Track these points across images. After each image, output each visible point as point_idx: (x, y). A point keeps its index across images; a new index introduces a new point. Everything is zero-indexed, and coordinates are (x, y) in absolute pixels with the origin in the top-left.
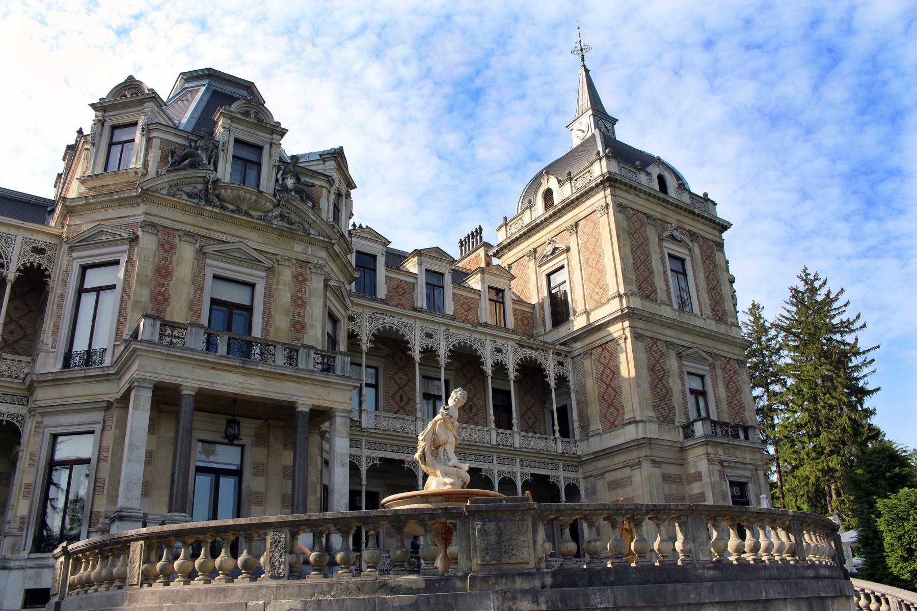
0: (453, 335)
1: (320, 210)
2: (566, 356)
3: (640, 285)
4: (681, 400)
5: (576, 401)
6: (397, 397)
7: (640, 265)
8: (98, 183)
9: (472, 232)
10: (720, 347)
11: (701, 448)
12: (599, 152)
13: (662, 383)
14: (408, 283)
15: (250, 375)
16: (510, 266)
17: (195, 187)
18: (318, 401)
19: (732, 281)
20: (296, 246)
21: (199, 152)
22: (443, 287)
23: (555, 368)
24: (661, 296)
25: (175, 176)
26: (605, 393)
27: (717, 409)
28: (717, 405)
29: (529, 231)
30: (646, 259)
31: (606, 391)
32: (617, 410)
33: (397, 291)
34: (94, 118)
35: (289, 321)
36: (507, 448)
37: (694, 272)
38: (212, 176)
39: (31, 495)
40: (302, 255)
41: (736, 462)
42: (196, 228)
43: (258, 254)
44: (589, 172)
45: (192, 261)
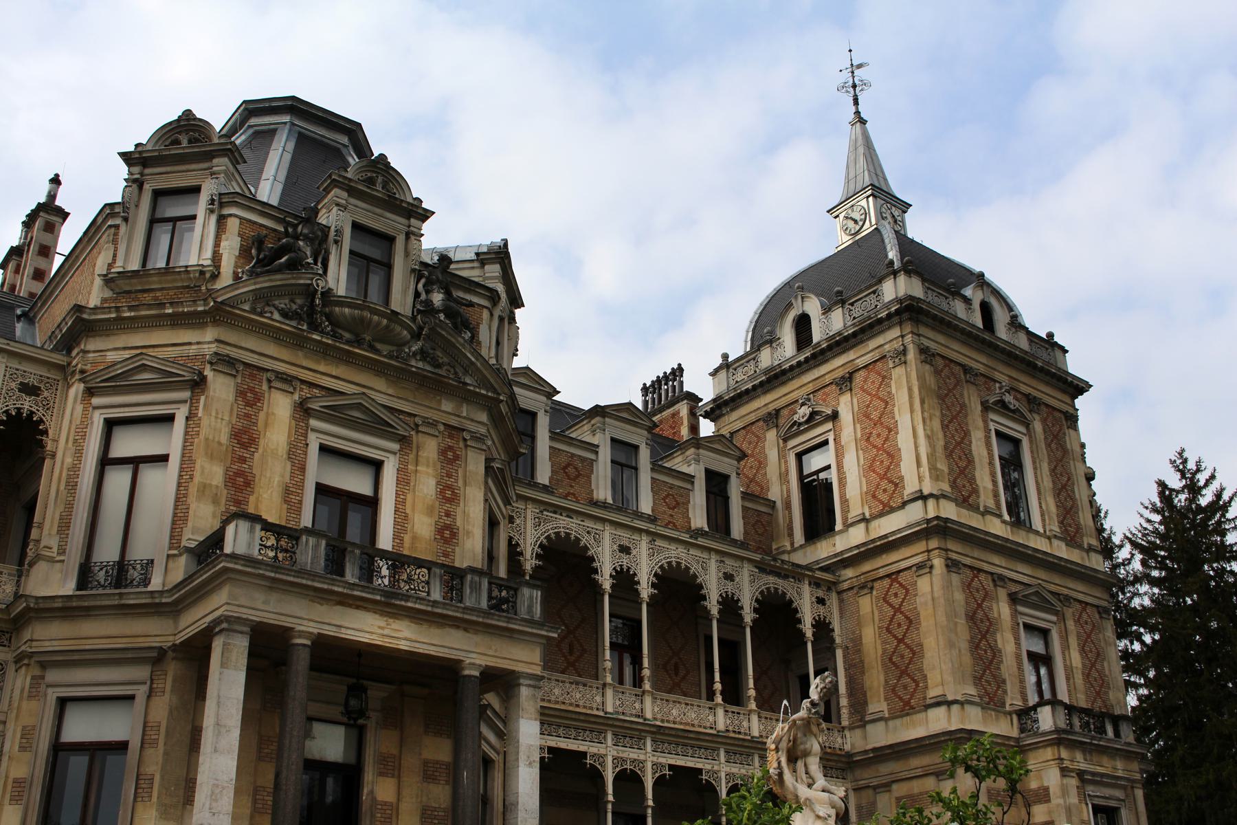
1: (479, 343)
2: (829, 589)
3: (954, 481)
4: (1015, 669)
5: (845, 662)
7: (955, 448)
9: (665, 373)
10: (1071, 585)
11: (1049, 750)
12: (892, 262)
13: (987, 641)
14: (583, 459)
15: (394, 616)
16: (732, 434)
17: (292, 301)
18: (494, 660)
19: (1090, 477)
20: (443, 401)
21: (301, 243)
22: (636, 469)
23: (812, 608)
24: (986, 500)
25: (264, 283)
26: (894, 652)
27: (1068, 685)
28: (1068, 679)
29: (769, 380)
30: (963, 439)
31: (896, 648)
32: (915, 681)
33: (566, 473)
34: (127, 177)
35: (433, 524)
36: (741, 736)
37: (1034, 462)
38: (321, 284)
39: (25, 798)
40: (453, 417)
41: (1102, 775)
42: (294, 368)
43: (389, 414)
44: (874, 292)
45: (288, 421)
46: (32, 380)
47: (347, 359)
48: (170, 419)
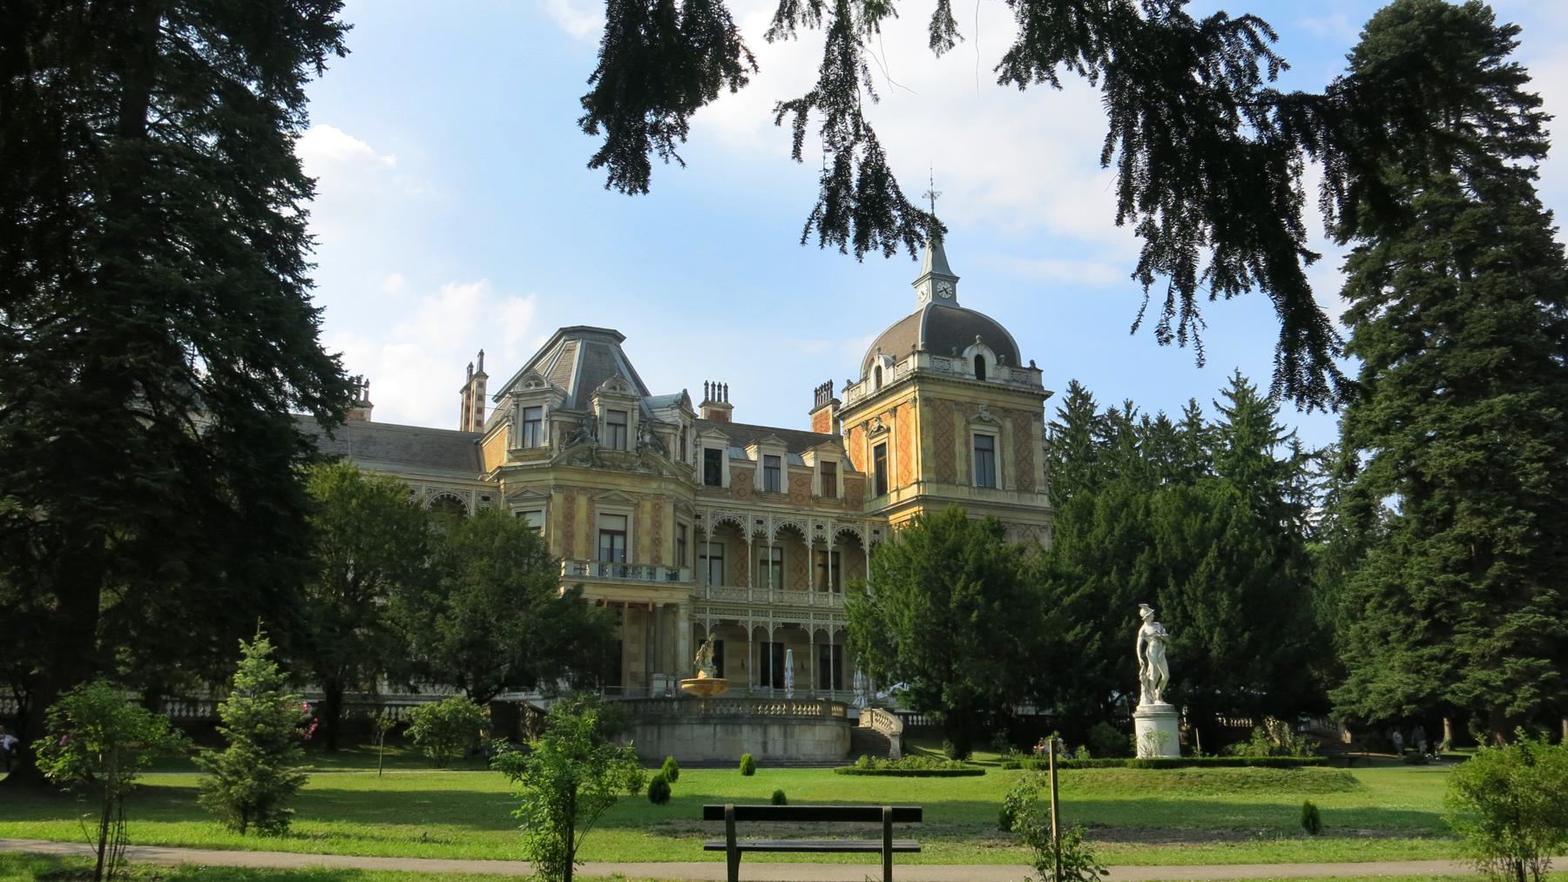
0: (780, 519)
6: (739, 566)
8: (521, 454)
22: (779, 469)
25: (571, 451)
46: (487, 495)
47: (610, 474)
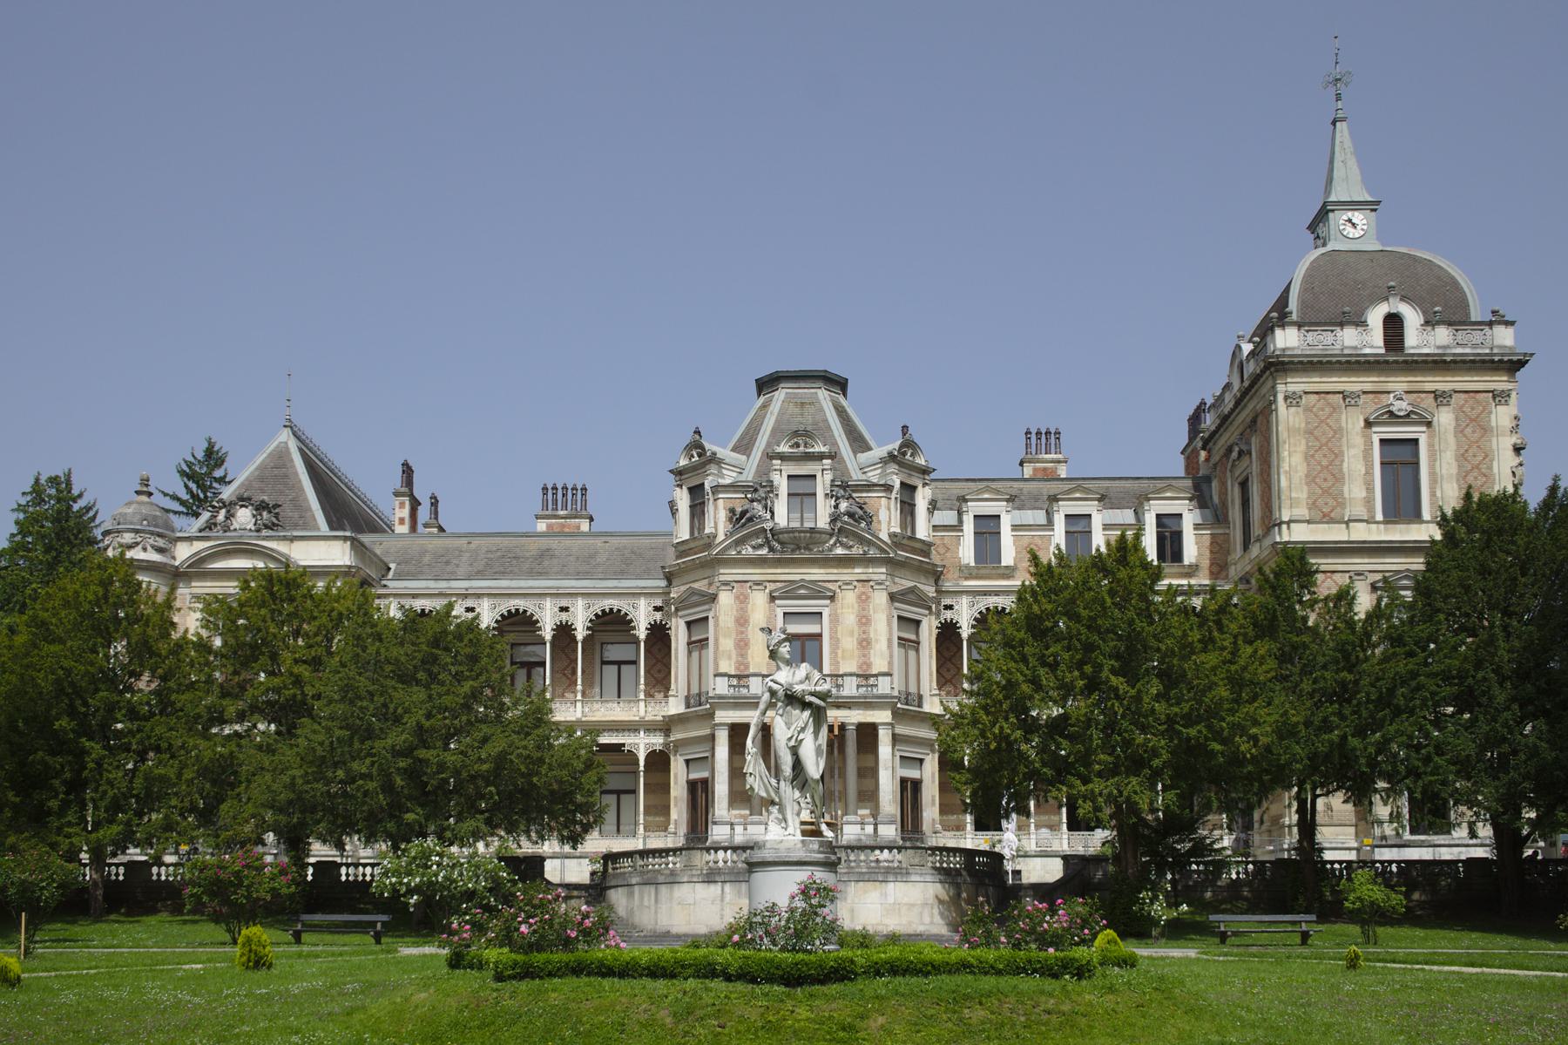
3: (1314, 503)
17: (758, 538)
48: (707, 618)
